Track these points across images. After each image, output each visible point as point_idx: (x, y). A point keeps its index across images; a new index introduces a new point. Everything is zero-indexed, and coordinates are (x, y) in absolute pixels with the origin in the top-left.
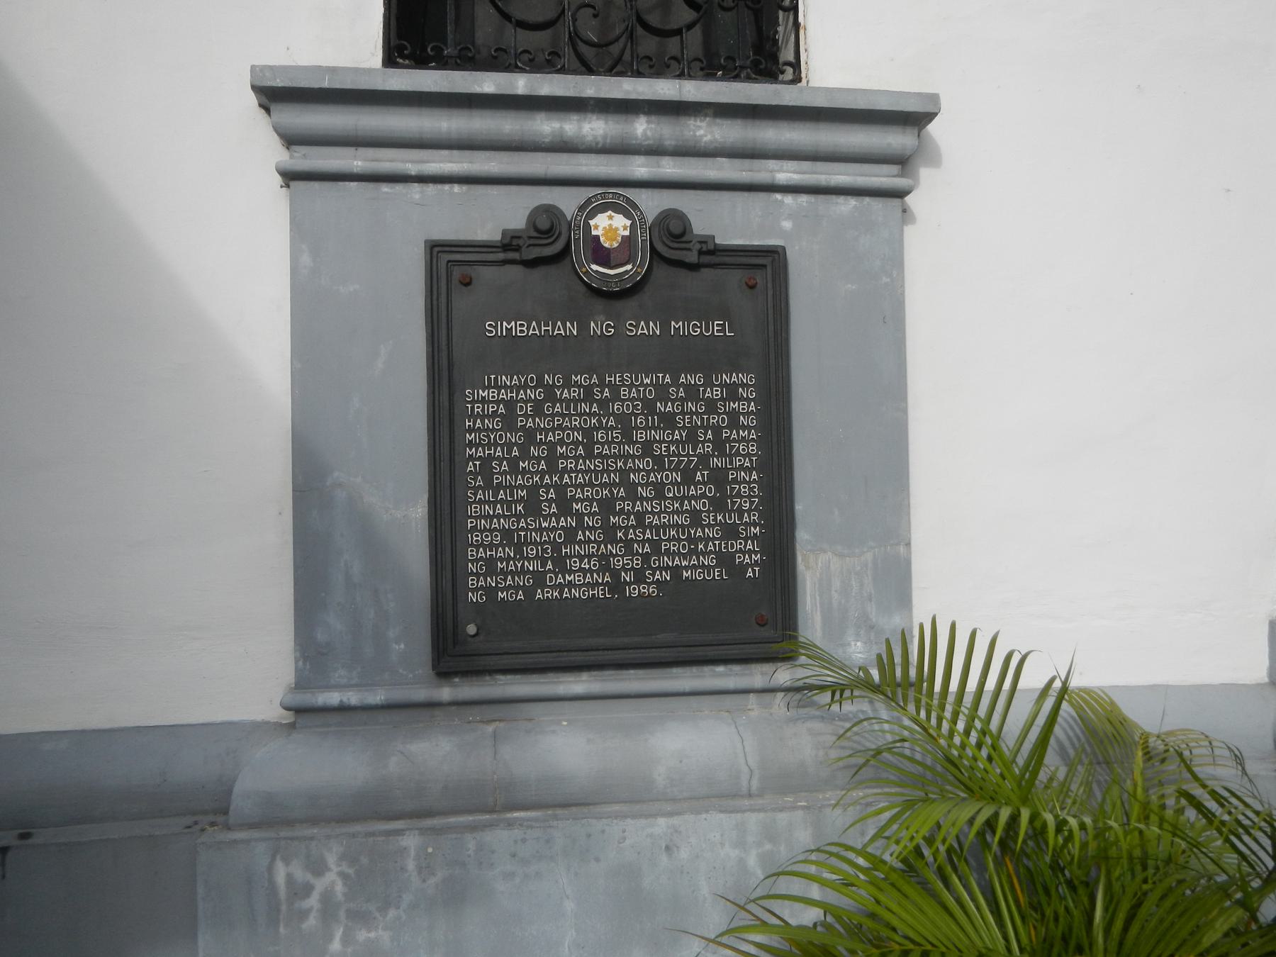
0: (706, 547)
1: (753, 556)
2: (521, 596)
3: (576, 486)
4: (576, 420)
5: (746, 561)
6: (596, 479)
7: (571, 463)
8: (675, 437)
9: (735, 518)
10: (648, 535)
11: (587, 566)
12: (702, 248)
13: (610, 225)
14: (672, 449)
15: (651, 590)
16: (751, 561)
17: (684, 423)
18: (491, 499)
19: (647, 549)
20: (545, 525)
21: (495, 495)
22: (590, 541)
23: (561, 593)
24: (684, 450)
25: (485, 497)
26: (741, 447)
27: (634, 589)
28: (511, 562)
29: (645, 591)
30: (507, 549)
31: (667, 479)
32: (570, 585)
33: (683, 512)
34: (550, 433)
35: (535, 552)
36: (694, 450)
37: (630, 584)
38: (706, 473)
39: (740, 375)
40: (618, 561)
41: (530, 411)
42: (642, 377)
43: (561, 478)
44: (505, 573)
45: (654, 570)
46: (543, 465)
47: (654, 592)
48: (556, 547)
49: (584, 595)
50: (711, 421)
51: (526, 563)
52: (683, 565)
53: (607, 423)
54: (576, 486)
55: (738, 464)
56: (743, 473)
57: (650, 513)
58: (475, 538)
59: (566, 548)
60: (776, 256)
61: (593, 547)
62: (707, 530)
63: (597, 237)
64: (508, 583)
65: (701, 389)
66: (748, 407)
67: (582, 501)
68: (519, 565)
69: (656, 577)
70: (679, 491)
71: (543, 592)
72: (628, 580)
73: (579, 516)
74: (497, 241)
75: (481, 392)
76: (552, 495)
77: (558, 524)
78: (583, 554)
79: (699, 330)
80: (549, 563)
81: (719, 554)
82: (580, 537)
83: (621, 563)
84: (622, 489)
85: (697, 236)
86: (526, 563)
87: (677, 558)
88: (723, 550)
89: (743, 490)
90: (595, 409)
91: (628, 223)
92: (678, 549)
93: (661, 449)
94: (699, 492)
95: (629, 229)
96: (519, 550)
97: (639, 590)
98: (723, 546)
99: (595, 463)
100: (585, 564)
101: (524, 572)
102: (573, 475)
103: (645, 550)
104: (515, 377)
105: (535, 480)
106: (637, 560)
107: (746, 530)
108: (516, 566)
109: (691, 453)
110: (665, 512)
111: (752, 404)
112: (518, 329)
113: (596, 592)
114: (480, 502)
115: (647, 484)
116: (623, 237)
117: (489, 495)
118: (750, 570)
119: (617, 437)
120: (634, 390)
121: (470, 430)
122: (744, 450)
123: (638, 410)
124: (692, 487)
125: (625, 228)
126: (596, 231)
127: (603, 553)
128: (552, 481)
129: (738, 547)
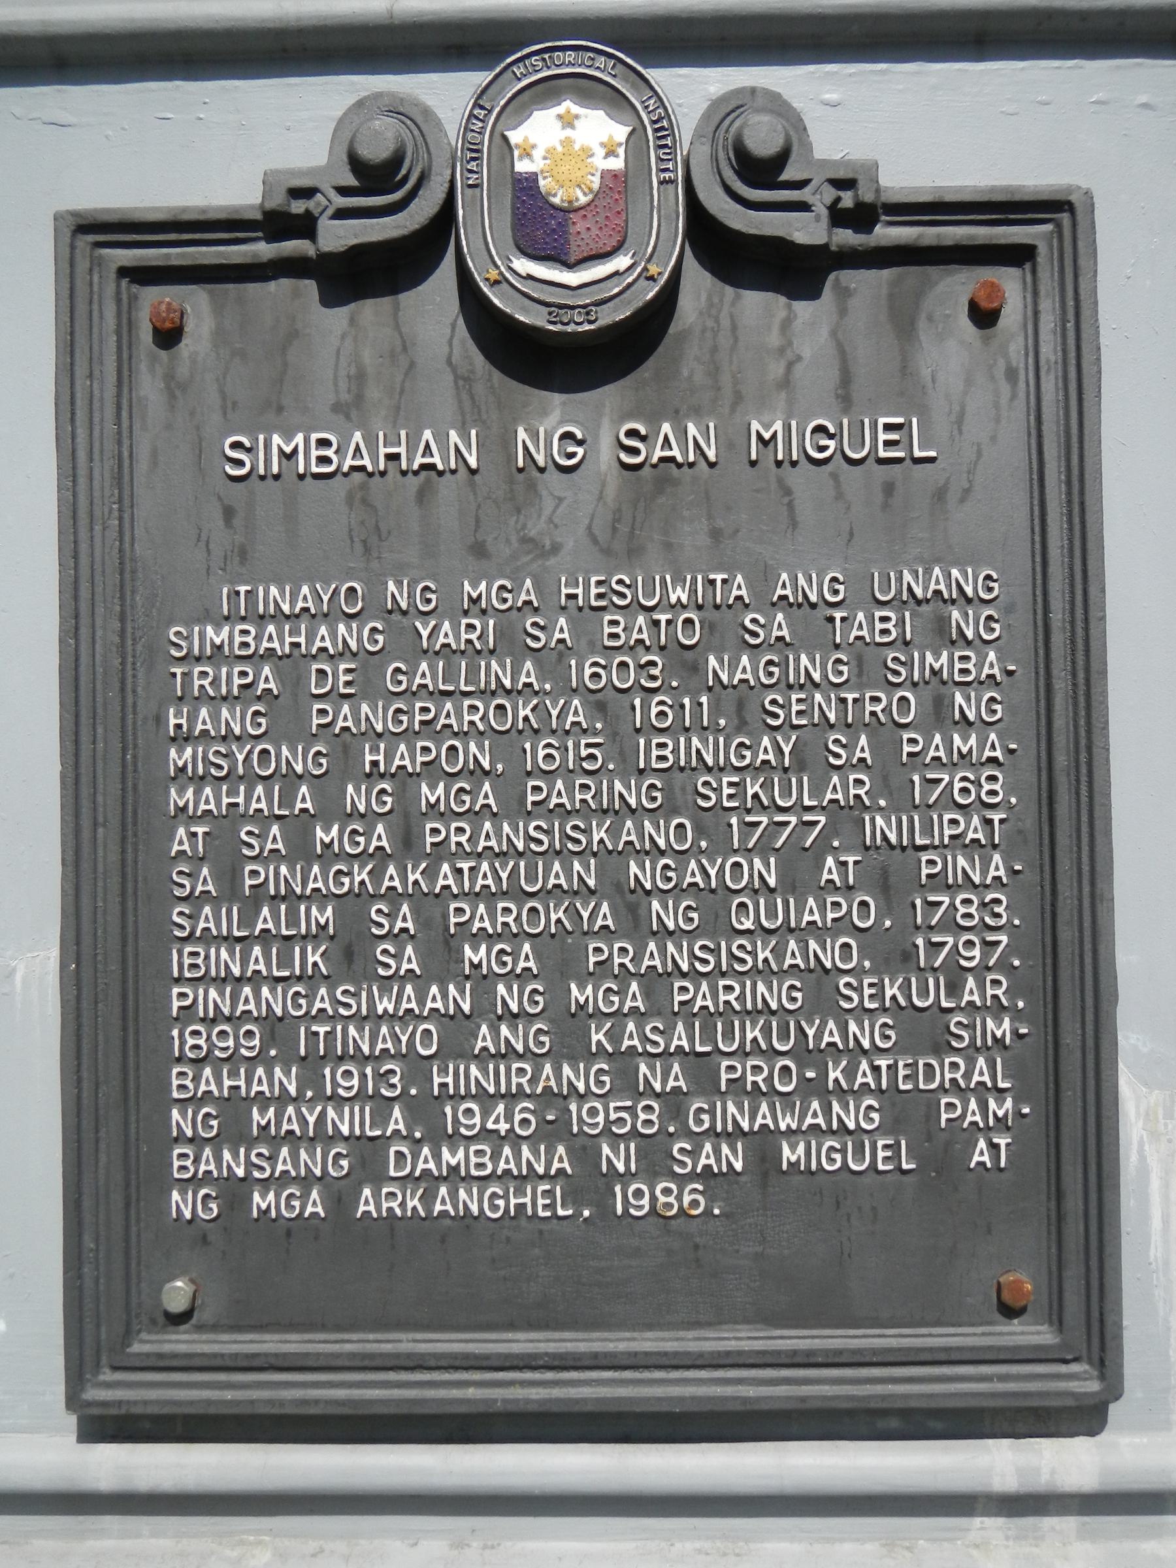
0: (850, 1073)
1: (992, 1104)
2: (315, 1205)
3: (474, 897)
4: (473, 708)
5: (969, 1119)
6: (532, 878)
7: (460, 830)
8: (762, 757)
9: (935, 994)
10: (680, 1039)
11: (503, 1127)
12: (838, 199)
13: (567, 142)
14: (750, 792)
15: (687, 1199)
16: (985, 1117)
17: (788, 716)
18: (237, 933)
19: (677, 1079)
20: (385, 1005)
21: (247, 920)
22: (510, 1054)
23: (428, 1198)
24: (786, 792)
25: (218, 925)
26: (957, 786)
27: (638, 1194)
28: (290, 1110)
29: (671, 1199)
30: (278, 1072)
31: (737, 878)
32: (454, 1176)
33: (783, 974)
34: (402, 747)
35: (355, 1082)
36: (817, 791)
37: (627, 1177)
38: (851, 860)
39: (955, 573)
40: (593, 1112)
41: (348, 684)
42: (663, 581)
43: (431, 873)
44: (274, 1140)
45: (697, 1139)
46: (381, 835)
47: (694, 1204)
48: (417, 1066)
49: (494, 1208)
50: (869, 708)
51: (331, 1113)
52: (783, 1127)
53: (561, 715)
54: (474, 897)
55: (947, 832)
56: (961, 862)
57: (684, 975)
58: (191, 1040)
59: (444, 1071)
60: (1065, 217)
61: (521, 1071)
62: (853, 1027)
63: (533, 178)
64: (280, 1168)
65: (838, 615)
66: (980, 666)
67: (491, 938)
68: (311, 1120)
69: (703, 1161)
70: (772, 914)
71: (376, 1195)
72: (621, 1168)
73: (483, 980)
74: (252, 207)
75: (210, 630)
76: (406, 919)
77: (421, 1002)
78: (491, 1090)
79: (832, 444)
80: (397, 1113)
81: (889, 1096)
82: (484, 1038)
83: (600, 1119)
84: (605, 908)
85: (824, 163)
86: (331, 1113)
87: (764, 1108)
88: (902, 1087)
89: (962, 910)
90: (529, 673)
91: (620, 132)
92: (769, 1080)
93: (718, 790)
94: (830, 916)
95: (621, 151)
96: (311, 1077)
97: (653, 1198)
98: (902, 1072)
99: (526, 832)
100: (497, 1121)
101: (323, 1137)
102: (465, 866)
103: (671, 1083)
104: (305, 590)
105: (357, 879)
106: (648, 1108)
107: (971, 1027)
108: (303, 1122)
109: (807, 802)
110: (731, 973)
111: (992, 656)
112: (315, 453)
113: (527, 1200)
114: (207, 938)
115: (679, 891)
116: (604, 174)
117: (230, 921)
118: (982, 1144)
119: (592, 757)
120: (641, 620)
121: (182, 738)
122: (965, 791)
123: (654, 678)
124: (811, 901)
125: (611, 153)
126: (526, 161)
127: (548, 1089)
128: (404, 879)
129: (948, 1076)
